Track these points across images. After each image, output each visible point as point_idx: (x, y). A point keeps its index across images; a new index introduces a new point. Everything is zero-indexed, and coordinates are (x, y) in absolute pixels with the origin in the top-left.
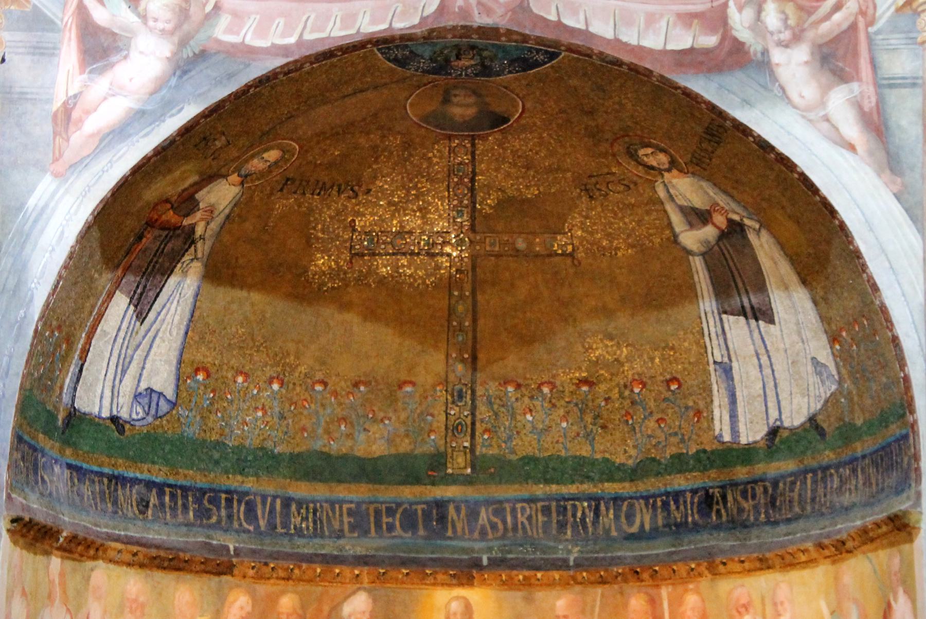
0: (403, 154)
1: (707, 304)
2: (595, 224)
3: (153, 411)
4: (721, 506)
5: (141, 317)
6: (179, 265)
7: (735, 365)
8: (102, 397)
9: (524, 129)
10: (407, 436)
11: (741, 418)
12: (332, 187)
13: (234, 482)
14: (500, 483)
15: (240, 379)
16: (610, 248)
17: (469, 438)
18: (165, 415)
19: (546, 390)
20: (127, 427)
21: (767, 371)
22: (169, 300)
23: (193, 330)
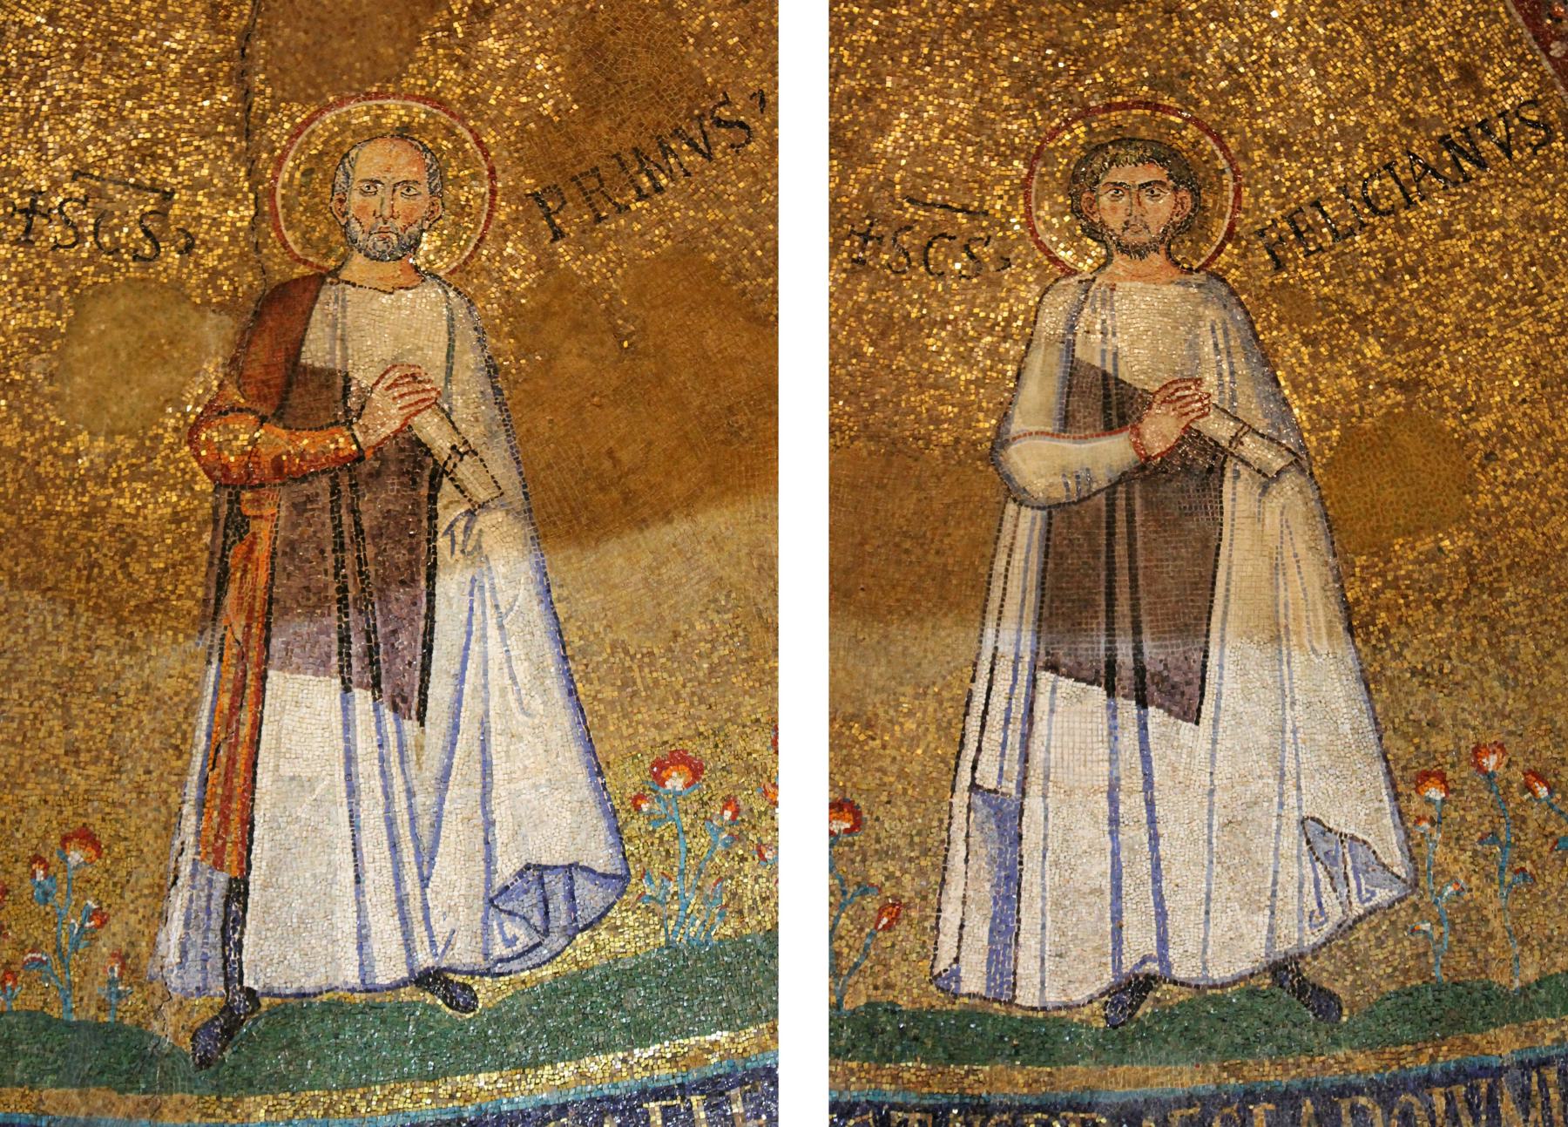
1: (1008, 635)
7: (1033, 803)
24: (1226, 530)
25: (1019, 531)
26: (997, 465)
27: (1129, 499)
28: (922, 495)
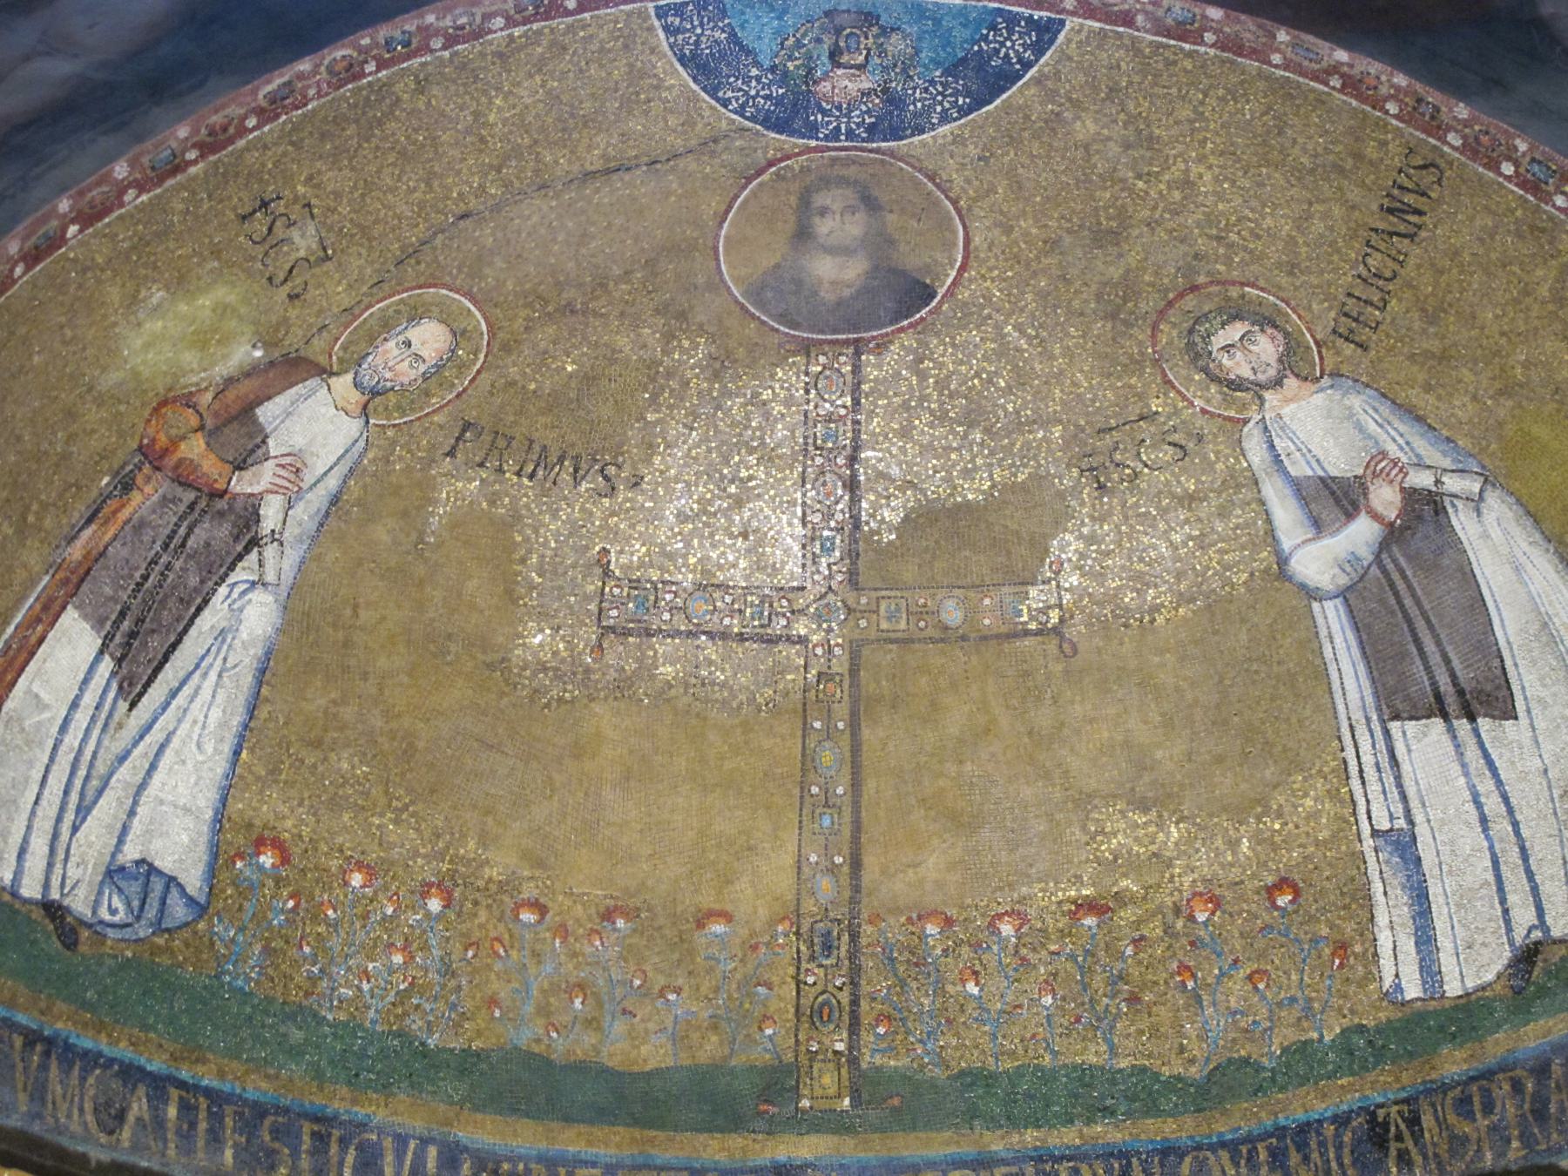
0: (710, 390)
2: (1108, 554)
3: (151, 913)
4: (1410, 1144)
5: (132, 687)
6: (223, 590)
7: (1422, 831)
9: (969, 315)
10: (715, 1027)
11: (1444, 942)
12: (561, 460)
13: (339, 1103)
14: (914, 1129)
15: (357, 879)
16: (1140, 609)
17: (845, 1035)
18: (179, 928)
19: (1007, 929)
20: (85, 934)
21: (1502, 827)
22: (197, 666)
23: (252, 750)
24: (1470, 554)
25: (1330, 621)
26: (1290, 579)
27: (1394, 561)
28: (1249, 625)
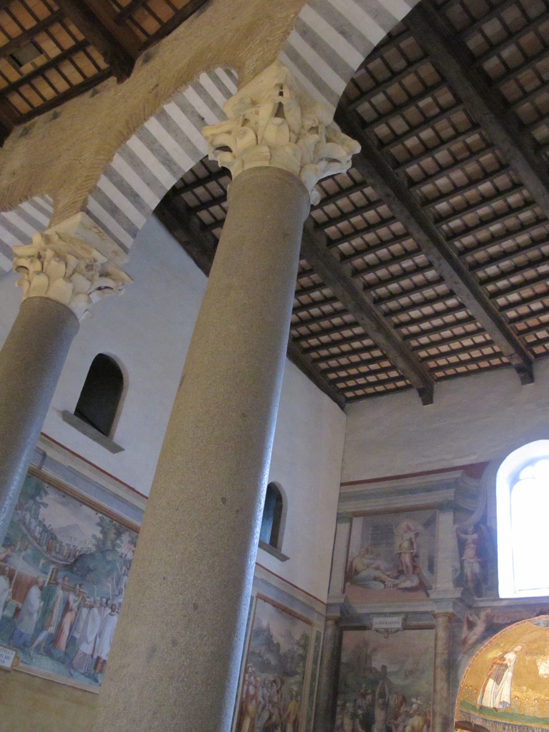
3: (505, 706)
8: (490, 703)
13: (529, 724)
